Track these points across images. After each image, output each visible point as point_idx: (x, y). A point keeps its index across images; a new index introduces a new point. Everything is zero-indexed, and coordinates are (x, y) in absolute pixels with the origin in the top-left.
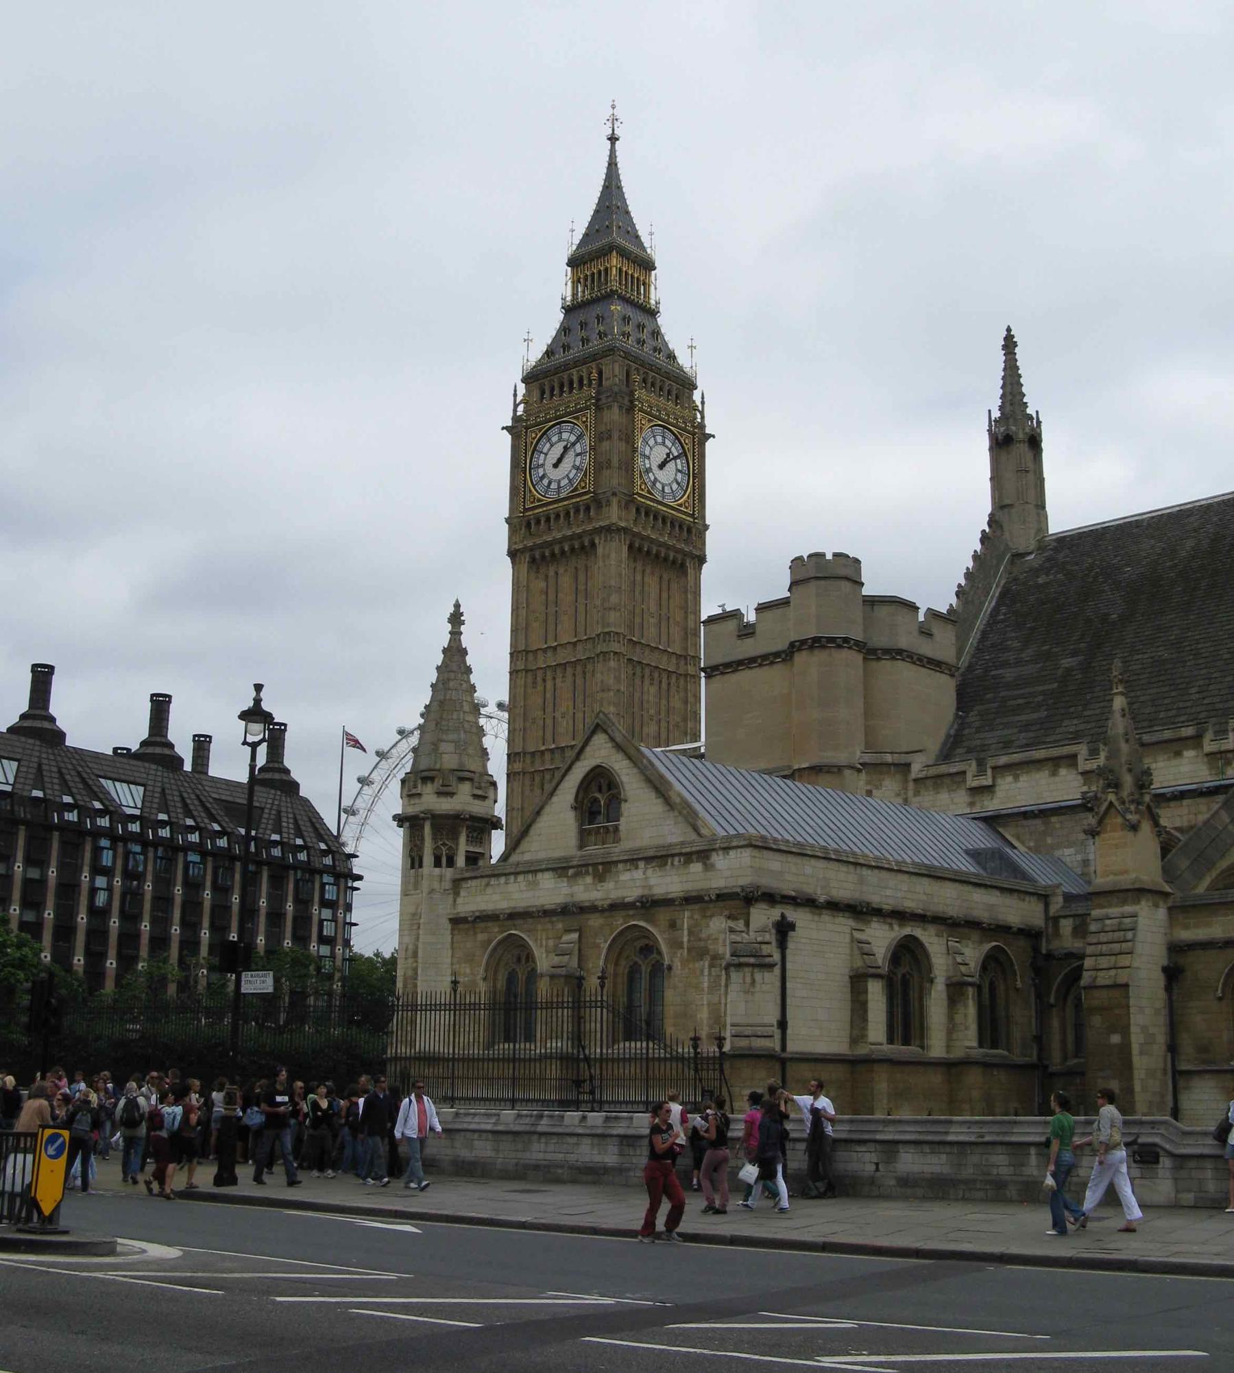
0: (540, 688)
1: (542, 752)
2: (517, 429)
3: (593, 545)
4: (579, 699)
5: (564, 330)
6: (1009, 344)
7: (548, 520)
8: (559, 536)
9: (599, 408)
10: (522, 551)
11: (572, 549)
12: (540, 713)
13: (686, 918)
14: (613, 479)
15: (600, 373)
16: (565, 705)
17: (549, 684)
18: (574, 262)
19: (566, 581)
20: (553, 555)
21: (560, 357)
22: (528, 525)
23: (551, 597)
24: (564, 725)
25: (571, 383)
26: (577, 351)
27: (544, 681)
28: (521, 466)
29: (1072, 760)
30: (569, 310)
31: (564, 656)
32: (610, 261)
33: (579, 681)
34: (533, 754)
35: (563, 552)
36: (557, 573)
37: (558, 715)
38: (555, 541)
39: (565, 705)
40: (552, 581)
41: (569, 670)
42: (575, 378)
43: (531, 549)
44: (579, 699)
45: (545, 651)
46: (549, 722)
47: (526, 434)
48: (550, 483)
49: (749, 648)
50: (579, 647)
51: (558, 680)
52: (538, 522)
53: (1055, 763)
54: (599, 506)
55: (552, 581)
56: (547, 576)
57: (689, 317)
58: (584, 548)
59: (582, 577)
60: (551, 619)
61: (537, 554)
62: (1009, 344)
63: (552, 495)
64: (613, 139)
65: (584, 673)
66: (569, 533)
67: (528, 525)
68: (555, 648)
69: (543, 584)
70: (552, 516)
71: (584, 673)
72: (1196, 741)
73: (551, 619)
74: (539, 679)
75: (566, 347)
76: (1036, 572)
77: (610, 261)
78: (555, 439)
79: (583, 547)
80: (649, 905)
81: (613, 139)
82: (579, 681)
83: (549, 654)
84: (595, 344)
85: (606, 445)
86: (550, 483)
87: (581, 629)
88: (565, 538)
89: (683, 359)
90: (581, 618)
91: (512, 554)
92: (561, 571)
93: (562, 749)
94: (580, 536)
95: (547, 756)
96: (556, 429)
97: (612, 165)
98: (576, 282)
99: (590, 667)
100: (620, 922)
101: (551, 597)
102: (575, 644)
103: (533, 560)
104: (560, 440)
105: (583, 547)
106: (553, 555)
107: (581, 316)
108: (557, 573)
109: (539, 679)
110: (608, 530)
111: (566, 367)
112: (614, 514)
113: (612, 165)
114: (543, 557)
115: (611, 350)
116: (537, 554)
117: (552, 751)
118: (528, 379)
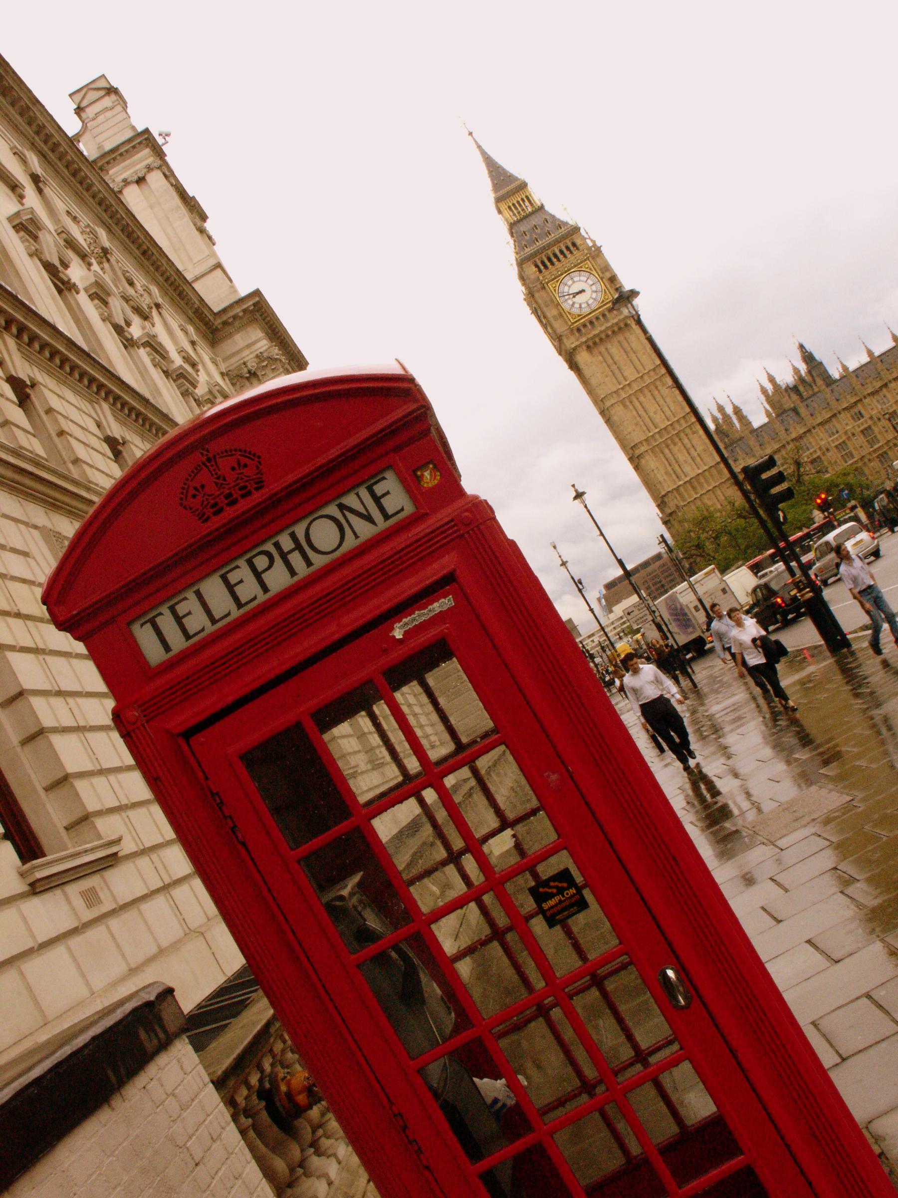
0: (631, 407)
1: (652, 436)
3: (626, 325)
4: (661, 402)
7: (591, 323)
8: (603, 328)
9: (593, 258)
10: (579, 346)
11: (614, 332)
12: (638, 418)
15: (574, 245)
16: (652, 407)
17: (637, 404)
20: (601, 340)
22: (579, 330)
23: (610, 361)
24: (658, 418)
25: (556, 256)
27: (631, 402)
31: (636, 387)
33: (656, 393)
34: (646, 440)
35: (607, 336)
36: (606, 349)
37: (652, 414)
38: (601, 332)
39: (652, 407)
40: (606, 355)
41: (646, 391)
43: (586, 342)
44: (661, 402)
45: (622, 388)
46: (647, 420)
48: (580, 305)
50: (646, 377)
51: (642, 399)
55: (606, 355)
56: (600, 353)
59: (625, 344)
60: (617, 372)
61: (591, 343)
63: (588, 310)
64: (470, 134)
65: (656, 388)
66: (609, 324)
67: (579, 330)
68: (629, 385)
69: (600, 358)
70: (594, 320)
71: (656, 388)
73: (617, 372)
74: (628, 403)
78: (570, 283)
79: (620, 329)
81: (470, 134)
82: (656, 393)
83: (628, 388)
86: (580, 305)
87: (640, 367)
88: (607, 328)
90: (637, 363)
92: (609, 346)
93: (665, 429)
94: (617, 324)
96: (568, 278)
97: (479, 147)
99: (658, 383)
101: (610, 361)
102: (642, 377)
103: (588, 347)
104: (574, 282)
105: (620, 329)
106: (601, 340)
108: (606, 349)
109: (628, 403)
111: (549, 246)
113: (479, 147)
114: (595, 343)
116: (591, 343)
117: (659, 433)
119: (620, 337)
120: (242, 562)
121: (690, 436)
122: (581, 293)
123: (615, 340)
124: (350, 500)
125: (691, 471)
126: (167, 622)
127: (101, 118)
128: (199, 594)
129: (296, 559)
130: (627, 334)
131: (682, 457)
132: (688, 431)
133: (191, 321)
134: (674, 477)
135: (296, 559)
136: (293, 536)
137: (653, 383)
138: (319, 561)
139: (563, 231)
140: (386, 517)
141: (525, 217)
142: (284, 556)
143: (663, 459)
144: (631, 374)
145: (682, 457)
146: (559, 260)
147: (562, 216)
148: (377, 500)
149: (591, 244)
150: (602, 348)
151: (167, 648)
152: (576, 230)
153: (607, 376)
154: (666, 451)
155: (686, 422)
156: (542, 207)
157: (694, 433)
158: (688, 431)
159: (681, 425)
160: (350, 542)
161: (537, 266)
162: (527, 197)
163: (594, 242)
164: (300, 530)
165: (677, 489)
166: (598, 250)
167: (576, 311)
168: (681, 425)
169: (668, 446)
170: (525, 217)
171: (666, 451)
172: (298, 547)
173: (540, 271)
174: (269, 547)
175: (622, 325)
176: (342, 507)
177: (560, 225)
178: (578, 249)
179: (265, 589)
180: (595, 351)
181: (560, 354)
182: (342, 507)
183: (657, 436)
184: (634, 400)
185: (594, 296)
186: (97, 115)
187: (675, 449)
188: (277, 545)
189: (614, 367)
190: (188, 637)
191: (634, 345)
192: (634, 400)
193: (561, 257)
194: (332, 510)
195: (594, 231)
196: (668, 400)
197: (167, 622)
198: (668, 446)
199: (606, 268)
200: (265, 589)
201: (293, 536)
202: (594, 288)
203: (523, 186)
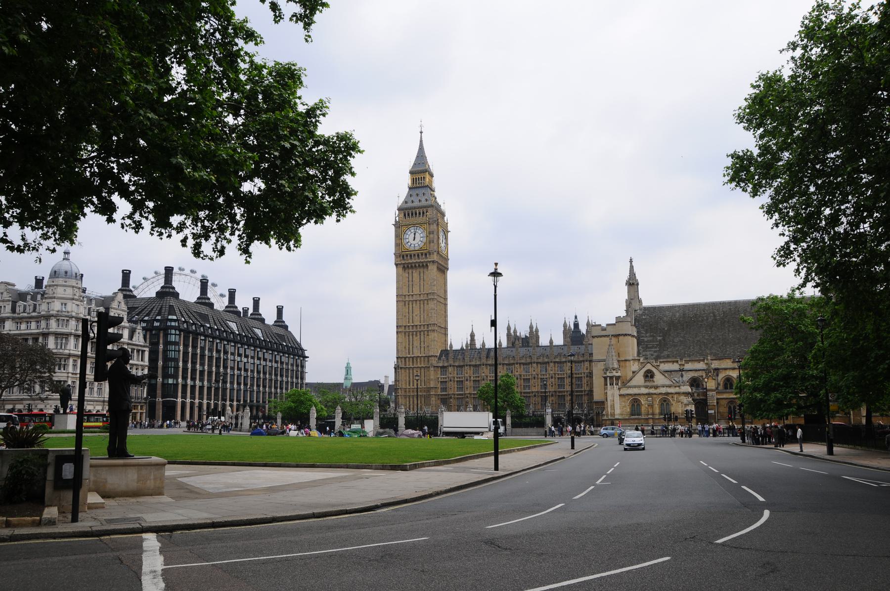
2: (397, 225)
5: (410, 195)
6: (631, 261)
13: (675, 396)
14: (433, 247)
16: (417, 312)
18: (411, 173)
19: (416, 275)
21: (410, 205)
24: (417, 319)
26: (416, 204)
28: (399, 237)
29: (677, 362)
30: (410, 188)
47: (400, 228)
49: (604, 333)
53: (673, 362)
54: (430, 254)
57: (444, 193)
58: (424, 266)
62: (631, 261)
63: (412, 249)
64: (421, 132)
72: (703, 360)
75: (412, 202)
76: (642, 315)
80: (667, 394)
81: (421, 132)
84: (424, 203)
85: (432, 236)
89: (442, 207)
91: (396, 265)
97: (421, 141)
98: (413, 180)
100: (661, 397)
103: (404, 267)
107: (417, 191)
110: (433, 262)
111: (415, 208)
112: (435, 257)
113: (421, 141)
115: (432, 206)
118: (399, 209)
119: (422, 270)
122: (416, 239)
123: (418, 270)
125: (417, 353)
130: (425, 270)
131: (416, 343)
137: (424, 301)
144: (416, 291)
145: (416, 343)
150: (410, 271)
165: (405, 358)
167: (407, 246)
187: (415, 338)
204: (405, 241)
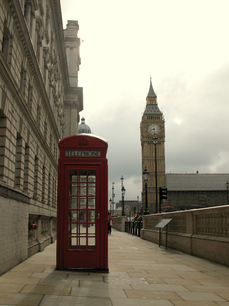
3: (160, 143)
15: (159, 117)
21: (149, 112)
22: (148, 138)
23: (151, 149)
25: (153, 117)
32: (152, 97)
42: (154, 117)
43: (149, 141)
45: (151, 157)
52: (150, 137)
54: (162, 138)
56: (150, 146)
61: (149, 142)
64: (151, 78)
65: (159, 162)
67: (148, 138)
68: (153, 157)
69: (150, 147)
71: (159, 162)
73: (151, 152)
77: (152, 97)
81: (151, 78)
83: (152, 158)
84: (157, 112)
95: (152, 173)
97: (151, 82)
99: (159, 161)
103: (148, 143)
104: (154, 126)
113: (151, 82)
114: (150, 143)
116: (149, 142)
120: (81, 151)
121: (160, 177)
122: (154, 129)
124: (95, 152)
126: (69, 153)
127: (71, 30)
128: (74, 152)
129: (86, 154)
130: (159, 145)
132: (160, 176)
133: (64, 86)
134: (151, 184)
135: (86, 154)
136: (87, 152)
138: (88, 156)
139: (159, 113)
140: (97, 156)
141: (152, 105)
142: (85, 153)
143: (150, 179)
146: (153, 119)
147: (161, 110)
148: (97, 153)
149: (163, 120)
150: (151, 145)
151: (68, 155)
152: (162, 114)
153: (149, 152)
154: (152, 178)
155: (161, 174)
156: (157, 105)
157: (161, 177)
158: (160, 176)
159: (159, 173)
160: (92, 156)
161: (148, 117)
162: (155, 100)
163: (164, 119)
164: (88, 152)
166: (164, 122)
168: (159, 173)
169: (153, 176)
170: (152, 105)
171: (152, 178)
172: (87, 153)
173: (148, 119)
174: (84, 152)
175: (159, 142)
176: (93, 152)
177: (159, 111)
178: (159, 119)
179: (81, 155)
180: (149, 145)
181: (141, 140)
182: (93, 152)
183: (152, 173)
184: (152, 161)
185: (157, 132)
186: (71, 28)
188: (85, 152)
189: (151, 151)
190: (71, 155)
191: (159, 149)
192: (152, 161)
193: (154, 118)
194: (92, 152)
195: (166, 117)
196: (159, 166)
197: (69, 153)
198: (153, 176)
199: (163, 127)
200: (81, 155)
201: (87, 152)
202: (158, 130)
203: (156, 97)
204: (149, 130)
